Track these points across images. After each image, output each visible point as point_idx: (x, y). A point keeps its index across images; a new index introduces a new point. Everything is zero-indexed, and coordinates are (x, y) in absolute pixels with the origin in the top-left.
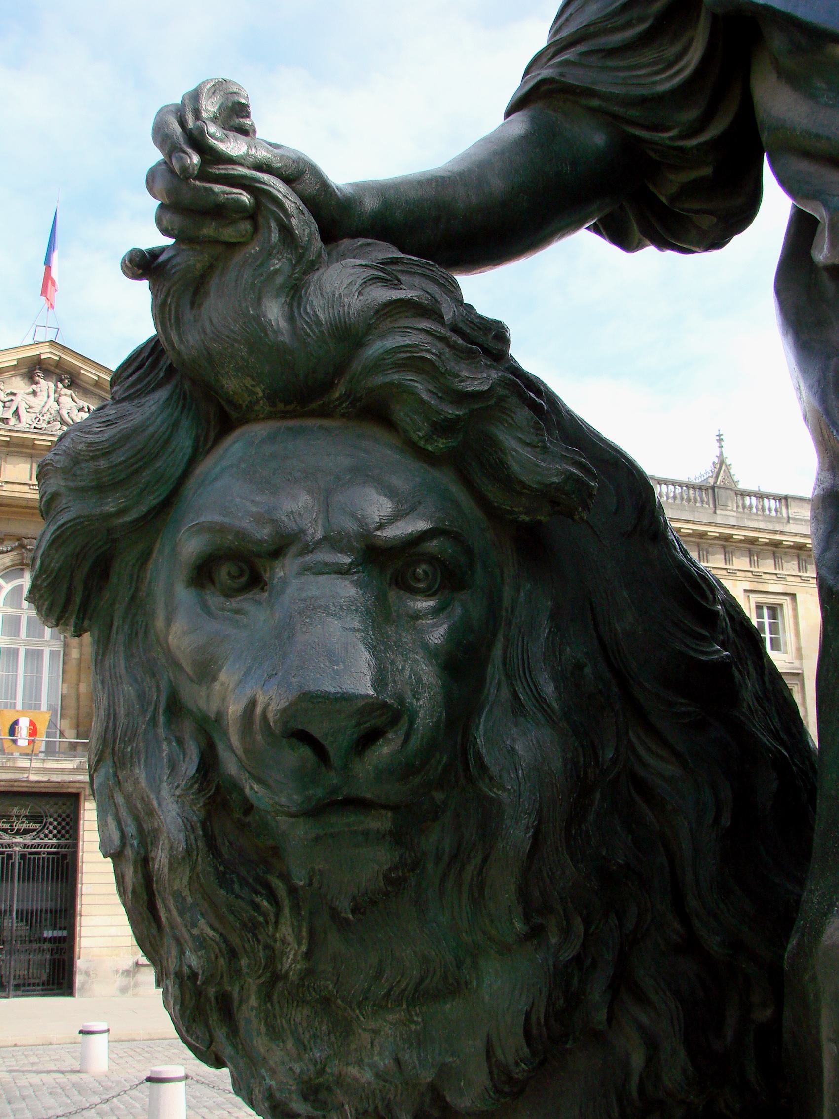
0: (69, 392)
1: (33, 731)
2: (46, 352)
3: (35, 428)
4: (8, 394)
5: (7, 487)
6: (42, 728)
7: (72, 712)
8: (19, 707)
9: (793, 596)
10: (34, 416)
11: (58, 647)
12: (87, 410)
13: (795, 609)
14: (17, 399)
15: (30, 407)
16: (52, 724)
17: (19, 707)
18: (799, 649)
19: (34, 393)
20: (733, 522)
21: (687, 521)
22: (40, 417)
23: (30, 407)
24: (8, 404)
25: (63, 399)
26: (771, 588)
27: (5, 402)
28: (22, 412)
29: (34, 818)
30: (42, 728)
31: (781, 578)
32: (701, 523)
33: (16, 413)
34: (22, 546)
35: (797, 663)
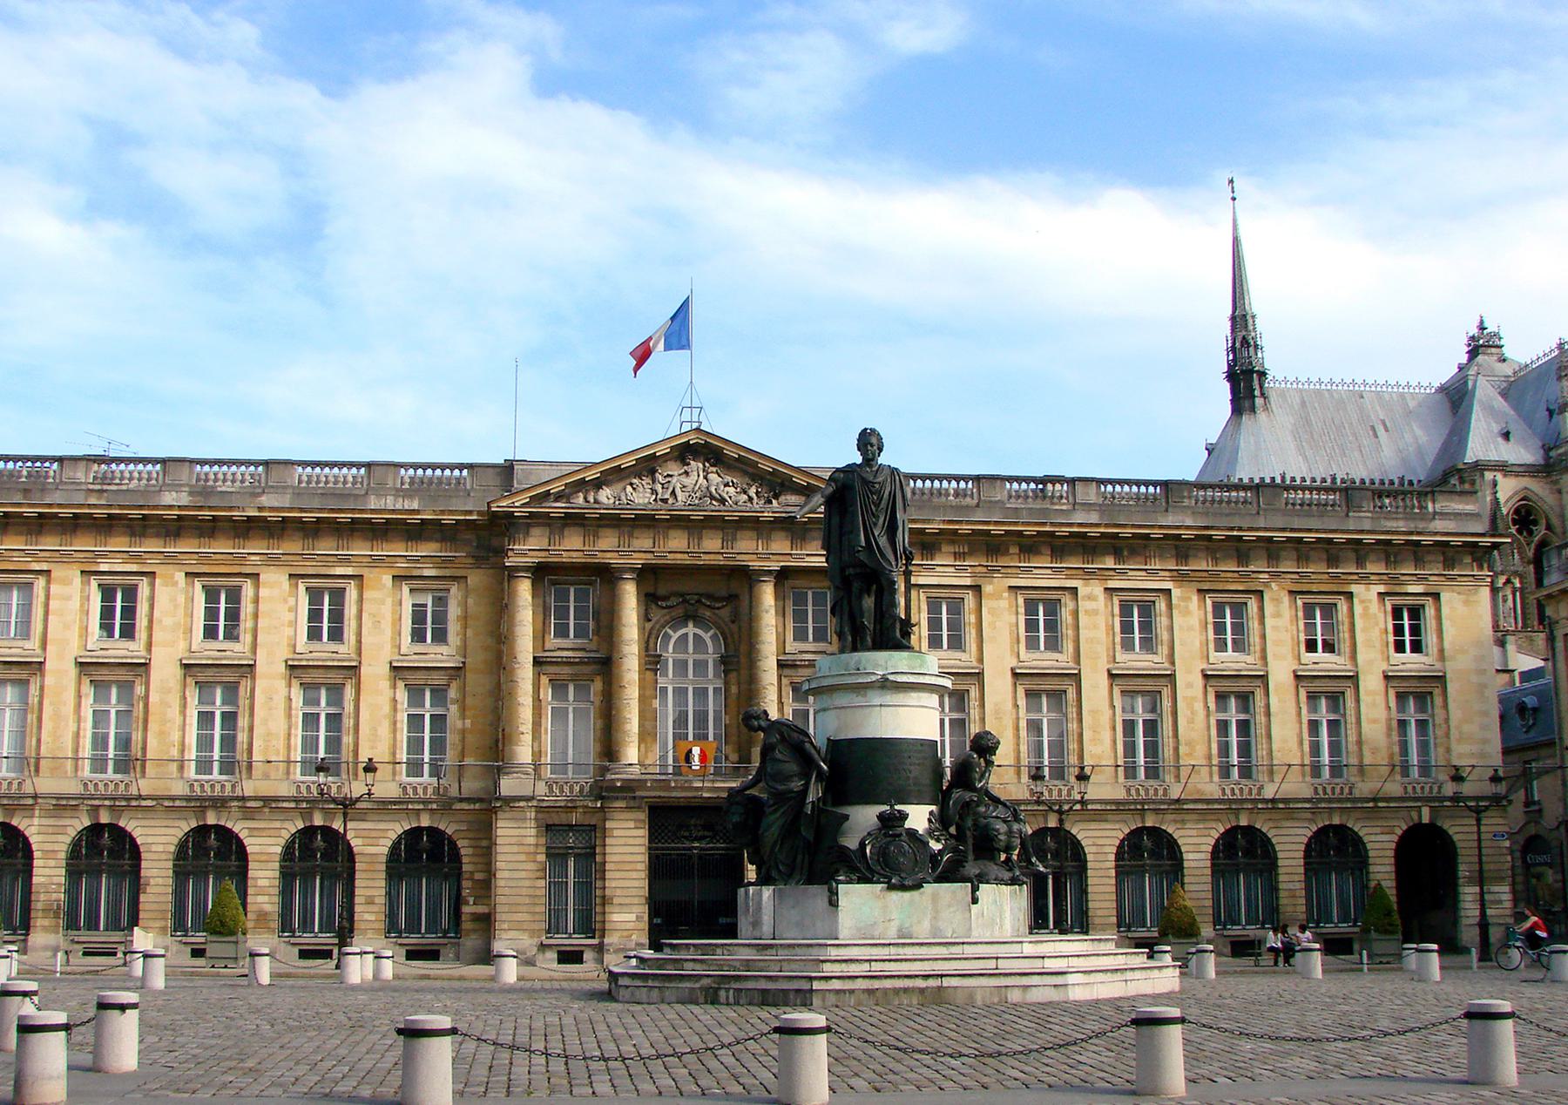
1: (703, 757)
2: (693, 439)
5: (670, 556)
6: (711, 755)
7: (734, 738)
8: (691, 738)
9: (1436, 596)
11: (720, 684)
13: (1438, 610)
14: (674, 480)
16: (719, 749)
17: (691, 738)
18: (1441, 651)
19: (686, 473)
20: (1367, 527)
21: (1310, 530)
25: (711, 476)
26: (1411, 589)
28: (678, 491)
29: (705, 827)
30: (711, 755)
31: (1421, 579)
32: (1325, 531)
33: (673, 492)
34: (685, 601)
35: (1438, 665)
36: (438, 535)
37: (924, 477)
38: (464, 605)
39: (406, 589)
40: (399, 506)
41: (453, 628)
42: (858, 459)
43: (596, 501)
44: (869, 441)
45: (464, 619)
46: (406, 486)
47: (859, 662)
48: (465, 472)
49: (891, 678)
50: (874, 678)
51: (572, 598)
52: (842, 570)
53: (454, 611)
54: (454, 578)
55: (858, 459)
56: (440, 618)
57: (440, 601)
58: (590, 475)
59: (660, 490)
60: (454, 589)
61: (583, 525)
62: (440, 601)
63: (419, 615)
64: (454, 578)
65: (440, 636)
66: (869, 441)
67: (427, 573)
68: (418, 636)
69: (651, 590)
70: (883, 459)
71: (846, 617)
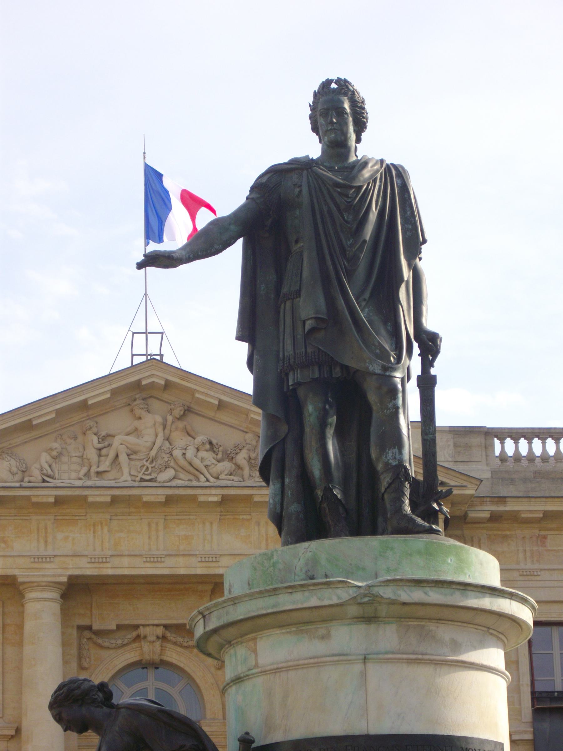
0: (180, 424)
3: (142, 480)
4: (104, 438)
10: (139, 464)
12: (208, 446)
14: (116, 442)
15: (135, 452)
19: (136, 432)
22: (147, 464)
23: (135, 452)
24: (104, 452)
27: (100, 450)
28: (123, 458)
37: (516, 434)
42: (312, 148)
47: (314, 561)
49: (388, 593)
50: (344, 595)
52: (282, 379)
55: (312, 148)
59: (92, 454)
69: (85, 622)
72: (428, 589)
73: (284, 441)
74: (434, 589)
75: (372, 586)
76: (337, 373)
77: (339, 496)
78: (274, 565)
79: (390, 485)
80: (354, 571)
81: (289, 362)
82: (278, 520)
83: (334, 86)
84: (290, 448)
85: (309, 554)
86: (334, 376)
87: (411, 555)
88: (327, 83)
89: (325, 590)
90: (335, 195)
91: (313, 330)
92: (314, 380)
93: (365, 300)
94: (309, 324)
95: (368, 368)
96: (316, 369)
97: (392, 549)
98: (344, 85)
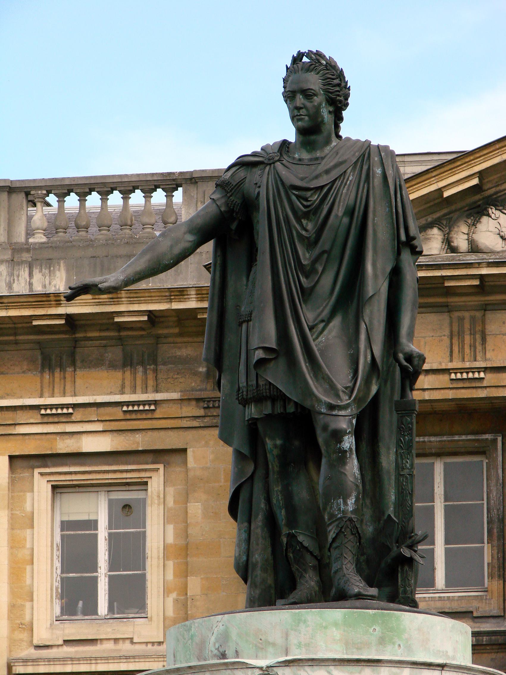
36: (115, 353)
38: (179, 517)
39: (41, 485)
40: (20, 288)
41: (157, 575)
43: (474, 248)
44: (317, 90)
45: (183, 552)
46: (40, 238)
48: (178, 196)
51: (439, 490)
53: (157, 533)
54: (158, 455)
56: (129, 552)
57: (127, 512)
58: (454, 184)
60: (156, 483)
61: (447, 308)
62: (127, 512)
63: (76, 546)
64: (158, 455)
65: (129, 597)
66: (317, 90)
67: (90, 444)
68: (76, 597)
70: (357, 125)
71: (259, 521)
72: (332, 668)
73: (251, 478)
74: (339, 667)
75: (271, 667)
76: (291, 409)
77: (306, 544)
78: (192, 638)
79: (334, 540)
80: (262, 646)
81: (243, 395)
82: (244, 571)
83: (305, 59)
84: (258, 486)
85: (222, 628)
86: (287, 411)
87: (326, 628)
88: (300, 55)
89: (224, 671)
90: (294, 198)
91: (261, 362)
92: (268, 416)
93: (323, 321)
94: (259, 354)
95: (314, 406)
96: (269, 404)
97: (305, 621)
98: (317, 57)
